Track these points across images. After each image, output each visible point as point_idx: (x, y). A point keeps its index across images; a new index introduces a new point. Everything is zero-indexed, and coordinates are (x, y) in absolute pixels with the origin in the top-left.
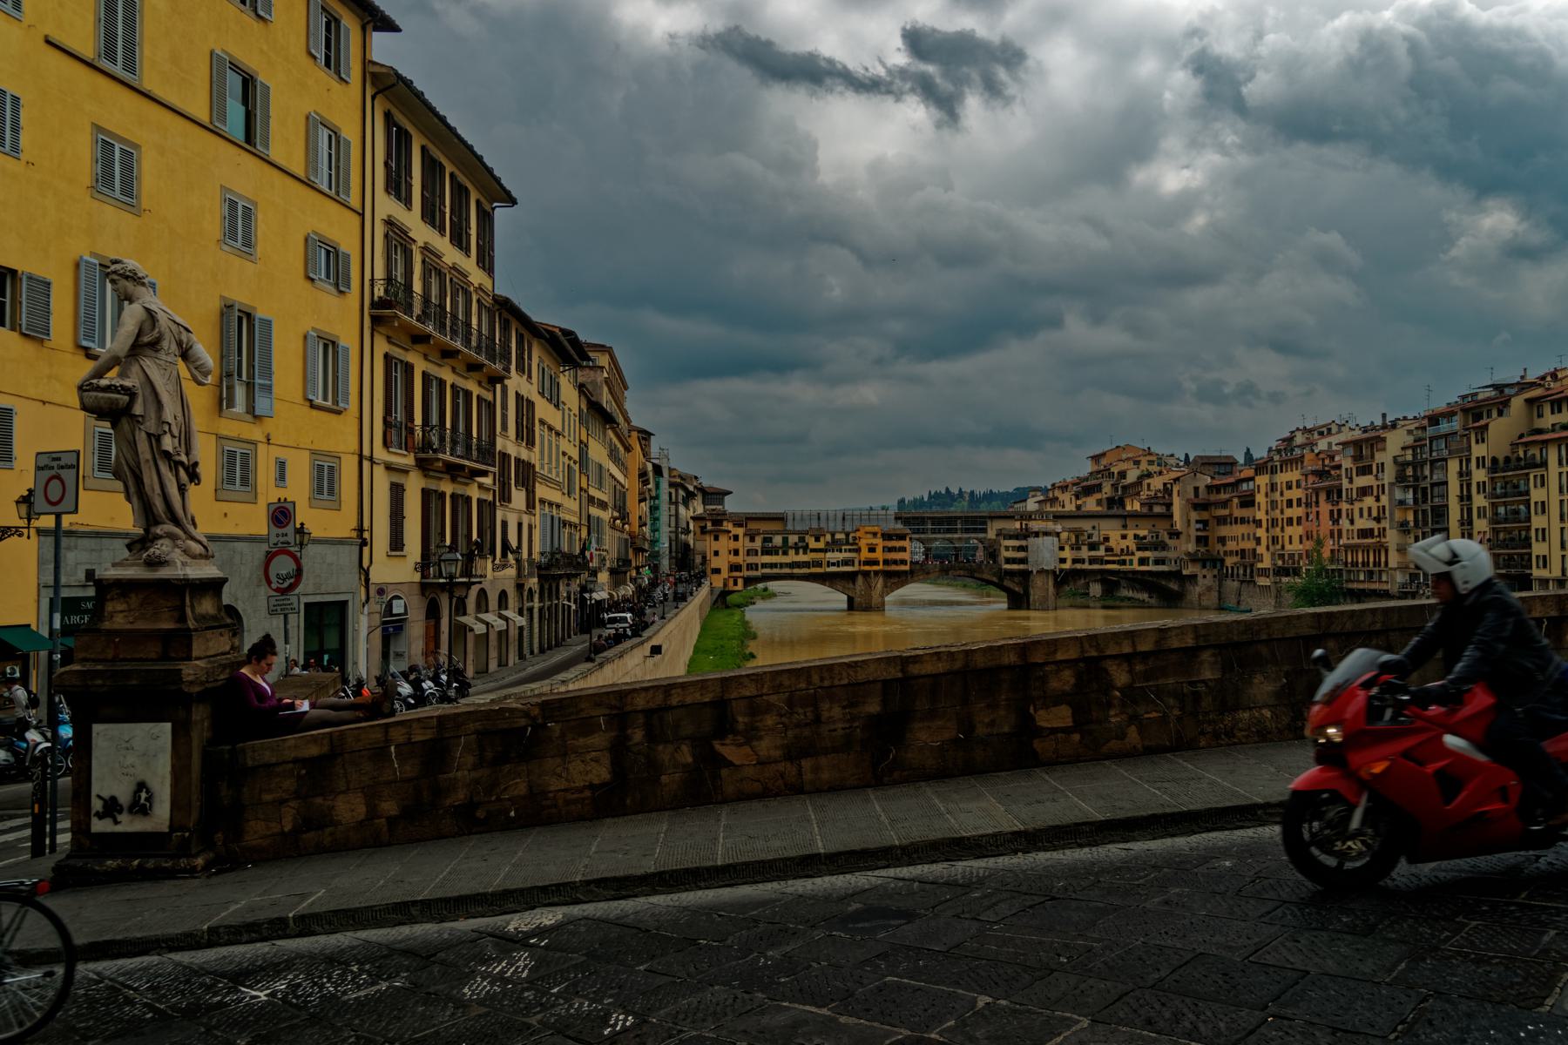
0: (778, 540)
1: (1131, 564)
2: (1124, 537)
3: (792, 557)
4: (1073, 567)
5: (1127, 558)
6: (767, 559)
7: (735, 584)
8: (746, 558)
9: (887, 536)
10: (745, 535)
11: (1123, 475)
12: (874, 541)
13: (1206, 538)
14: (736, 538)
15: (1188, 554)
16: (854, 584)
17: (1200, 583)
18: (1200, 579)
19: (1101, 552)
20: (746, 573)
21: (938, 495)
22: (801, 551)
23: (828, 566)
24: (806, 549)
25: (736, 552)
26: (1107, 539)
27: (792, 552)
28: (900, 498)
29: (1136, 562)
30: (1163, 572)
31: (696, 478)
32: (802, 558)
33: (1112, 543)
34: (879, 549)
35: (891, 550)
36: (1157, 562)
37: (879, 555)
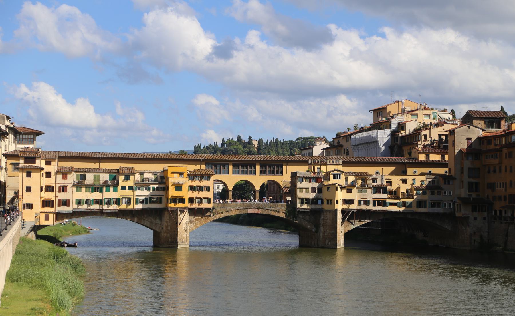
2: (405, 181)
4: (359, 208)
7: (47, 218)
8: (58, 194)
9: (192, 176)
10: (57, 173)
11: (401, 126)
12: (181, 181)
13: (477, 184)
14: (48, 175)
15: (460, 198)
16: (161, 219)
21: (230, 143)
22: (111, 189)
23: (137, 203)
25: (50, 189)
26: (390, 183)
28: (197, 143)
30: (438, 214)
32: (111, 194)
33: (394, 188)
34: (185, 188)
36: (433, 205)
37: (186, 194)
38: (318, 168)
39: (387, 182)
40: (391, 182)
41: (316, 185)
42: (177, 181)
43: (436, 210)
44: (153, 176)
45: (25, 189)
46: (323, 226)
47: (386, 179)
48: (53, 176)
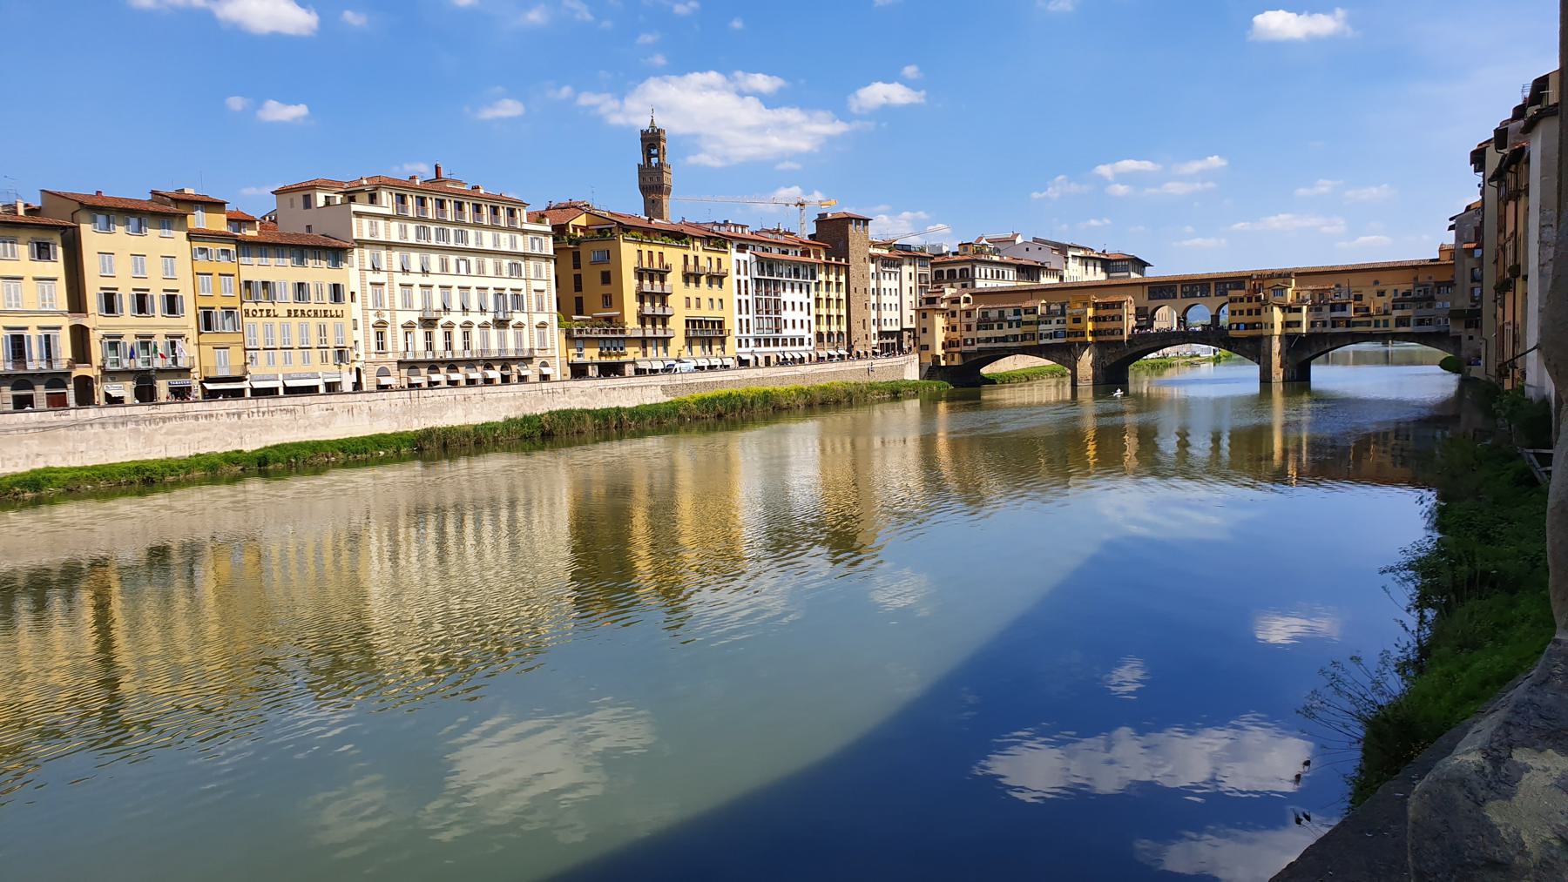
0: (994, 314)
1: (1386, 323)
2: (1381, 294)
3: (1007, 331)
4: (1313, 331)
5: (1381, 318)
6: (983, 334)
7: (953, 359)
17: (1464, 347)
18: (1464, 340)
19: (1350, 312)
20: (965, 348)
22: (1014, 324)
23: (1041, 339)
24: (1019, 323)
25: (954, 329)
26: (1358, 297)
27: (1006, 325)
29: (1392, 323)
31: (1084, 249)
32: (1015, 331)
35: (1104, 319)
36: (1420, 322)
38: (1260, 284)
39: (1355, 296)
40: (1361, 295)
41: (1254, 305)
42: (1074, 311)
43: (1432, 329)
44: (1059, 307)
45: (921, 330)
46: (1264, 355)
47: (1355, 292)
48: (958, 314)
